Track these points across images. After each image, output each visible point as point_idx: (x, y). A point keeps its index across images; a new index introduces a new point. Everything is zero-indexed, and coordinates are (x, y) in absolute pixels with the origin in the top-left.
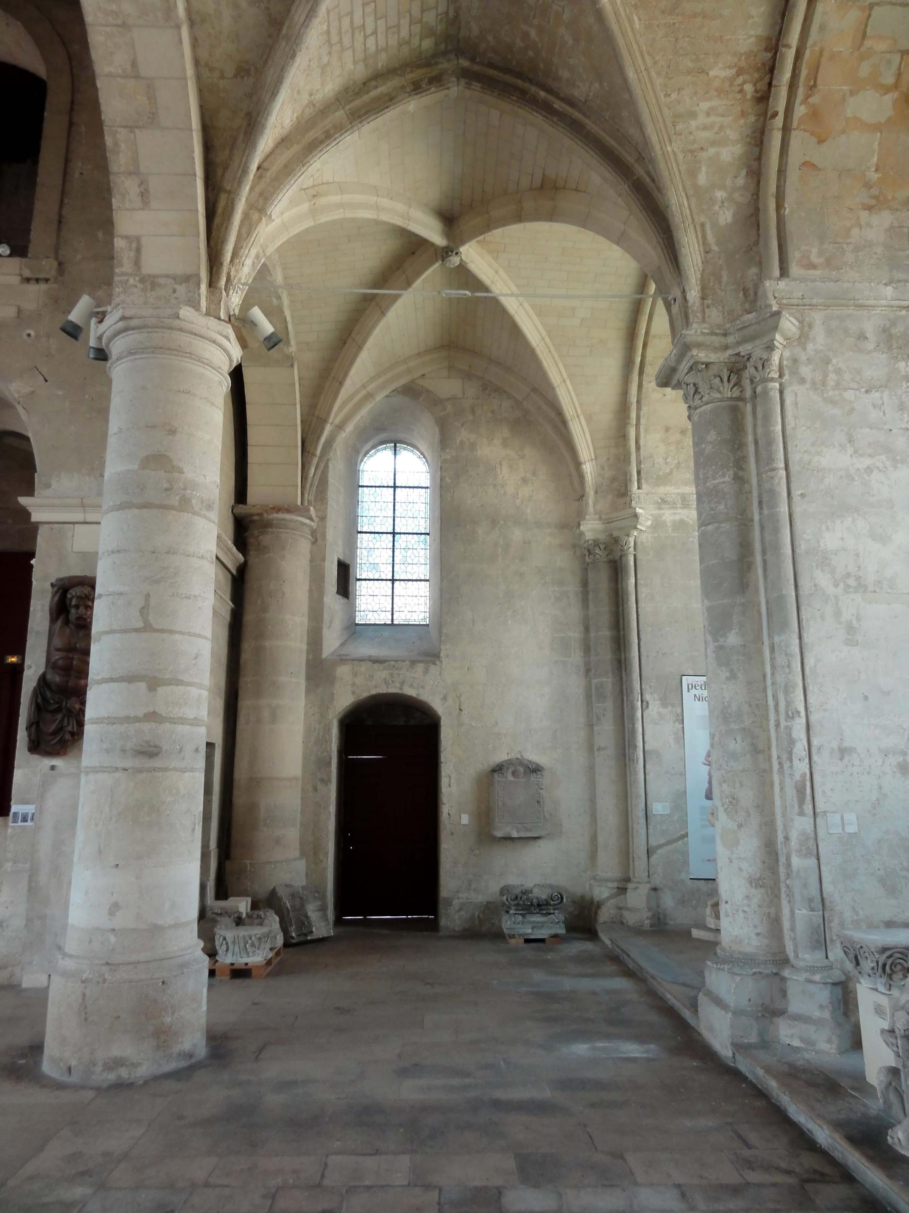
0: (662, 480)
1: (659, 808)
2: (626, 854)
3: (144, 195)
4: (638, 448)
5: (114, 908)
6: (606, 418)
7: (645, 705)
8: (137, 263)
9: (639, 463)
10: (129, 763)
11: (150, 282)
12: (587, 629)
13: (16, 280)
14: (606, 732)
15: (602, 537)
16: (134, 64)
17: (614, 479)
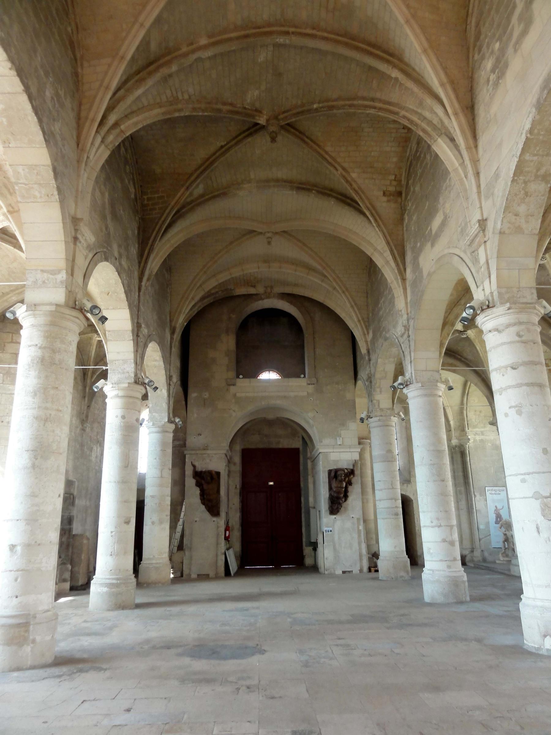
0: (475, 427)
1: (482, 527)
2: (472, 541)
3: (381, 392)
4: (467, 416)
5: (395, 547)
6: (456, 408)
7: (475, 496)
8: (379, 406)
9: (467, 421)
10: (394, 517)
11: (382, 410)
12: (454, 472)
13: (305, 384)
14: (463, 503)
15: (458, 444)
16: (384, 369)
17: (459, 426)
